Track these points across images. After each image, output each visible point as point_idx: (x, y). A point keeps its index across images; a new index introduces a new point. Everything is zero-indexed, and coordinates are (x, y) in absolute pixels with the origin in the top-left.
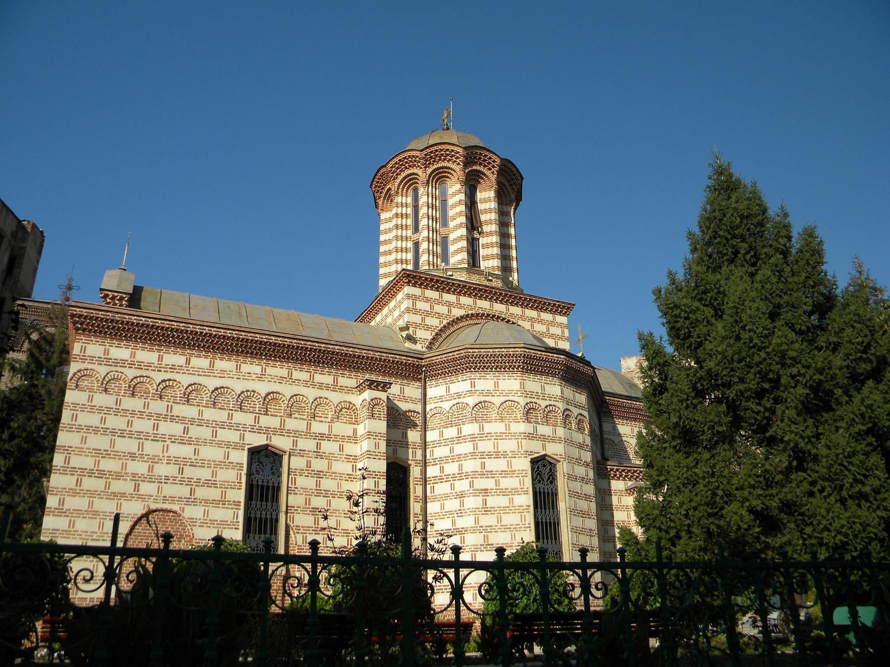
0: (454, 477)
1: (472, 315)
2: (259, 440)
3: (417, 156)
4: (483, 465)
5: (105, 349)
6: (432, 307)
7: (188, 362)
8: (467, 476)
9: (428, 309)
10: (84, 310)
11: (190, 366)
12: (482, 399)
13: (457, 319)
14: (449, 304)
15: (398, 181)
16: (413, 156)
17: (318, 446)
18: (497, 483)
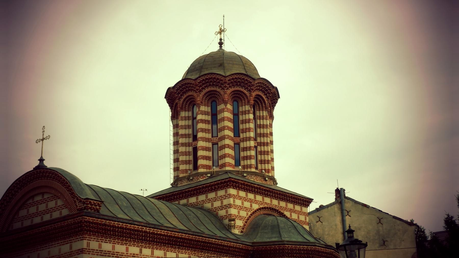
1: (263, 208)
3: (222, 80)
5: (99, 244)
6: (243, 203)
7: (141, 251)
9: (241, 204)
10: (91, 218)
11: (142, 254)
13: (255, 211)
14: (251, 201)
15: (203, 93)
16: (218, 79)
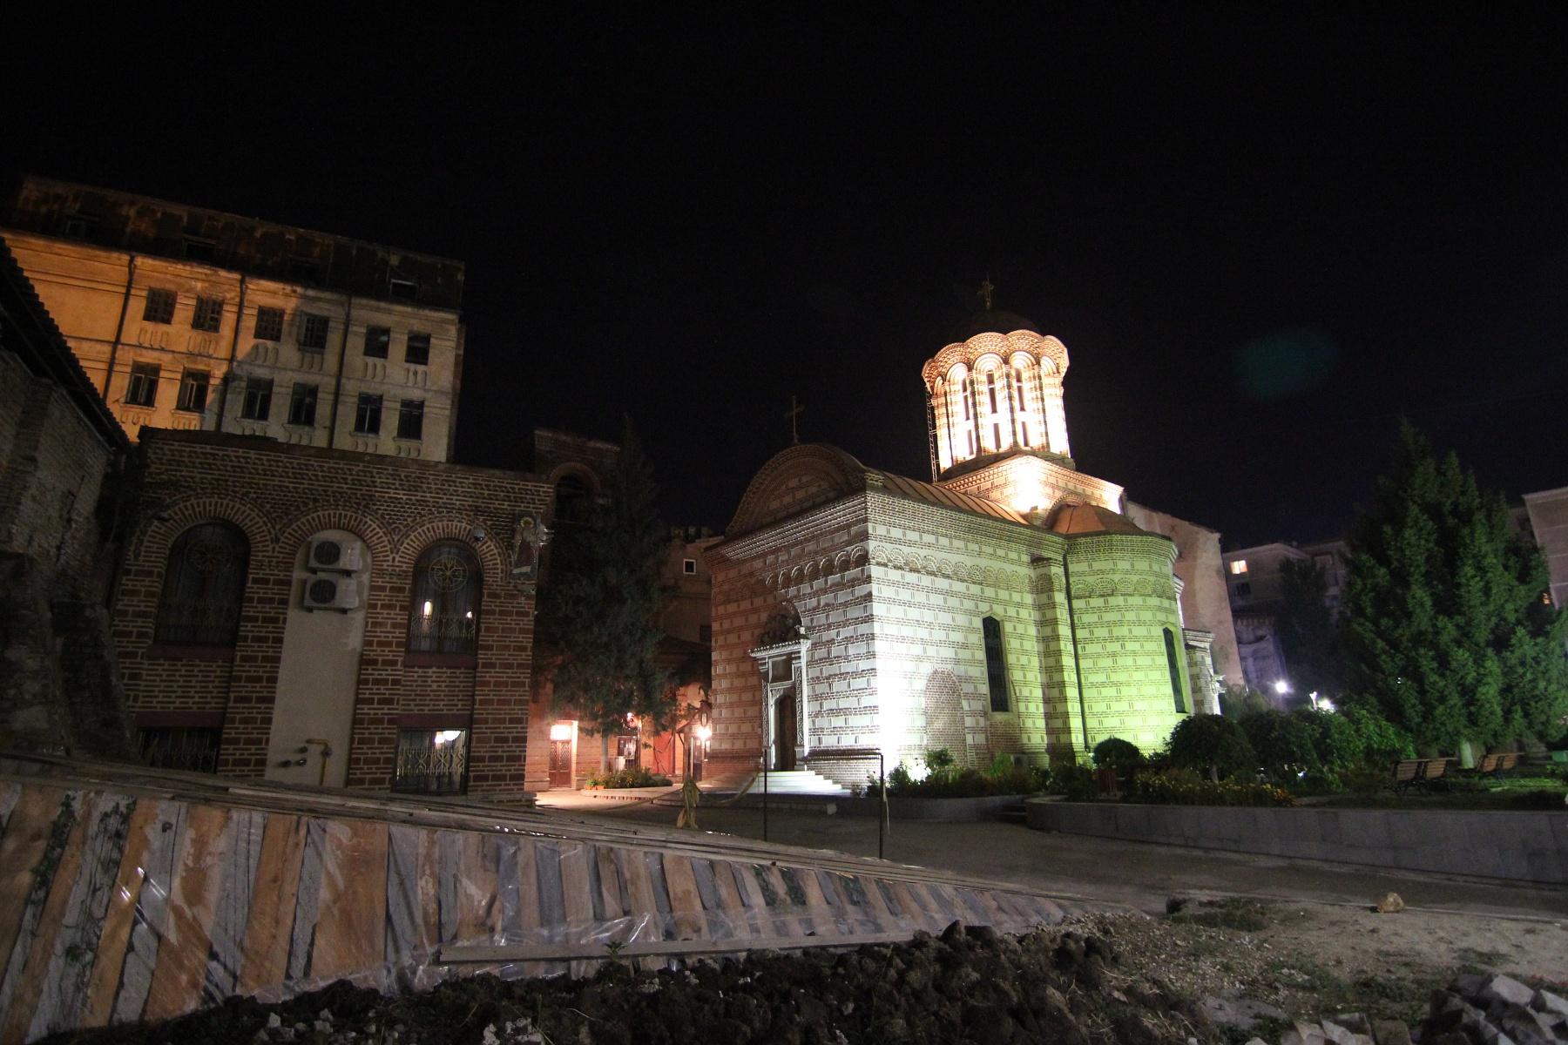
0: (1105, 640)
2: (984, 607)
4: (1130, 631)
8: (1118, 639)
12: (1123, 576)
17: (1018, 613)
18: (1142, 646)
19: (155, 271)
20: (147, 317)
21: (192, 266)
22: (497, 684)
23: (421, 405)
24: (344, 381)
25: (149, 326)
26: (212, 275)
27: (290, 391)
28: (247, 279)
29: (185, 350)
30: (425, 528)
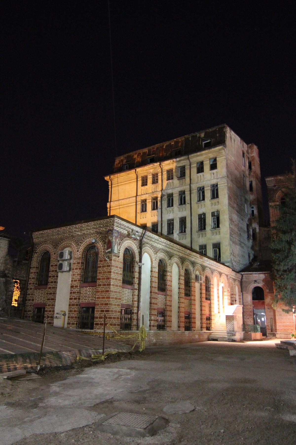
19: (142, 171)
20: (142, 186)
21: (148, 166)
22: (102, 292)
23: (217, 185)
24: (192, 185)
25: (143, 187)
26: (153, 166)
27: (178, 194)
28: (161, 163)
29: (151, 192)
30: (85, 242)
